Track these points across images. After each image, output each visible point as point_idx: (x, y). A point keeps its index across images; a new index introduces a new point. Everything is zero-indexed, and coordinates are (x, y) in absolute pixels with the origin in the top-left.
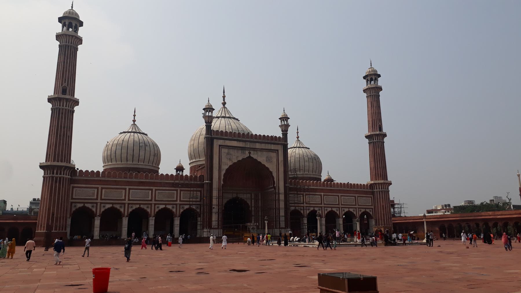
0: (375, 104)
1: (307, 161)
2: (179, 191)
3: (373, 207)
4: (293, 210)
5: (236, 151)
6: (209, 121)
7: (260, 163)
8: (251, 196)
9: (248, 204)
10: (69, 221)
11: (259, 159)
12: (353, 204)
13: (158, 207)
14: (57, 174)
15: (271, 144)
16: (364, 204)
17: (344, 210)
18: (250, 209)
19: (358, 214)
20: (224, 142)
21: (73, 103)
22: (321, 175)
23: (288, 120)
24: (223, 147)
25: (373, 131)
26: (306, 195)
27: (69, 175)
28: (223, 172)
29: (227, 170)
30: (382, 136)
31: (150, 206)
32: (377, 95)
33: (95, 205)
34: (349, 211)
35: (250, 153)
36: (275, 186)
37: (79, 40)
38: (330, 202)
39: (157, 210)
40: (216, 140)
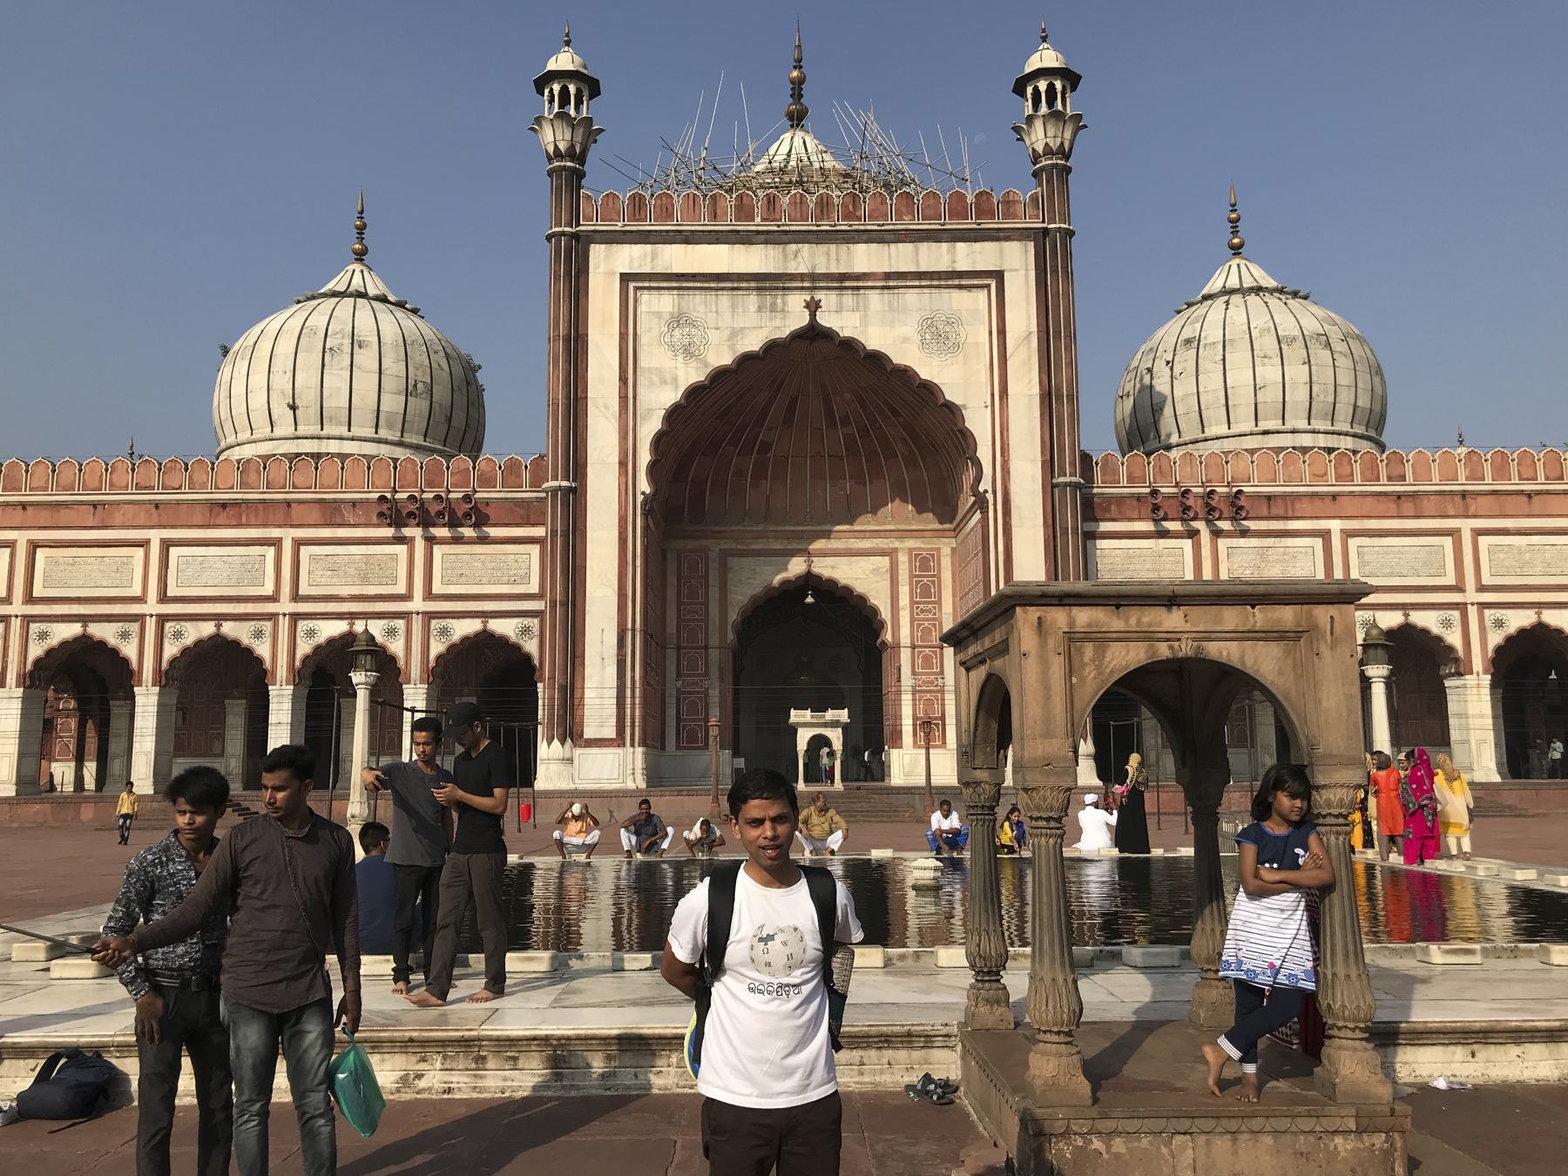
1: (1265, 357)
2: (420, 545)
5: (724, 299)
7: (877, 360)
9: (875, 611)
11: (874, 339)
13: (311, 633)
17: (1499, 624)
20: (654, 256)
22: (1383, 439)
24: (647, 284)
26: (1217, 534)
28: (650, 426)
29: (674, 415)
31: (267, 626)
34: (1540, 628)
35: (813, 306)
38: (1392, 575)
39: (304, 648)
40: (603, 246)
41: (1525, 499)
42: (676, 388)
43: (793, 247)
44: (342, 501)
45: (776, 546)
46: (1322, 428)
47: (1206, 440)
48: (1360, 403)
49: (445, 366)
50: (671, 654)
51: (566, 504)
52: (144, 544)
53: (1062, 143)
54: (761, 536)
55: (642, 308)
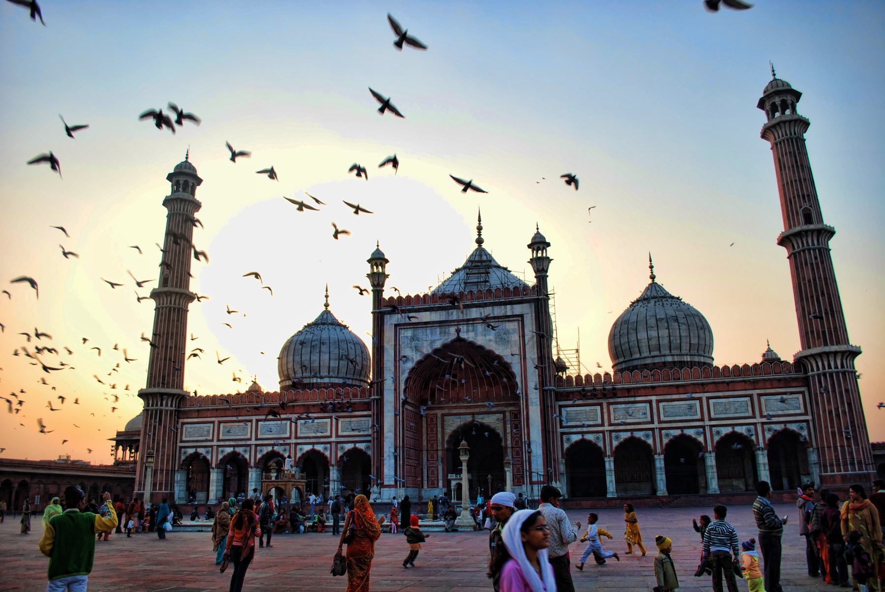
0: (788, 162)
3: (809, 418)
4: (576, 442)
5: (429, 331)
6: (378, 280)
7: (481, 348)
8: (505, 417)
9: (498, 434)
10: (179, 477)
11: (480, 341)
12: (746, 415)
13: (301, 449)
14: (153, 405)
15: (505, 304)
16: (780, 413)
17: (718, 433)
18: (503, 444)
19: (762, 438)
21: (178, 297)
22: (713, 356)
23: (548, 249)
25: (790, 227)
26: (609, 404)
27: (171, 406)
28: (404, 376)
29: (412, 370)
30: (815, 234)
31: (288, 447)
32: (792, 139)
33: (210, 449)
34: (734, 433)
35: (458, 331)
36: (518, 392)
37: (187, 203)
38: (676, 416)
39: (299, 454)
40: (389, 315)
41: (725, 385)
42: (413, 362)
43: (451, 311)
44: (311, 405)
45: (462, 411)
46: (675, 354)
47: (633, 360)
48: (692, 342)
49: (353, 347)
50: (425, 453)
51: (377, 404)
52: (251, 421)
53: (543, 268)
54: (456, 408)
55: (402, 335)
